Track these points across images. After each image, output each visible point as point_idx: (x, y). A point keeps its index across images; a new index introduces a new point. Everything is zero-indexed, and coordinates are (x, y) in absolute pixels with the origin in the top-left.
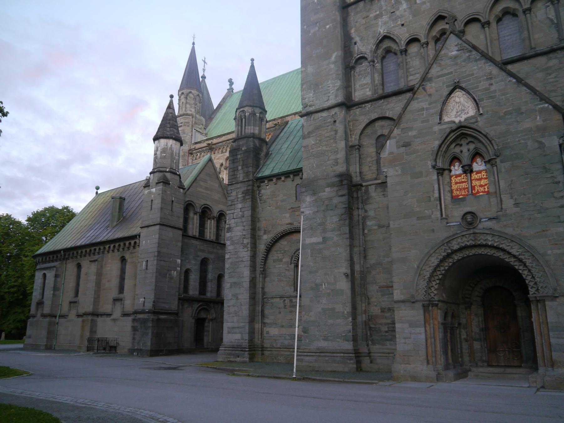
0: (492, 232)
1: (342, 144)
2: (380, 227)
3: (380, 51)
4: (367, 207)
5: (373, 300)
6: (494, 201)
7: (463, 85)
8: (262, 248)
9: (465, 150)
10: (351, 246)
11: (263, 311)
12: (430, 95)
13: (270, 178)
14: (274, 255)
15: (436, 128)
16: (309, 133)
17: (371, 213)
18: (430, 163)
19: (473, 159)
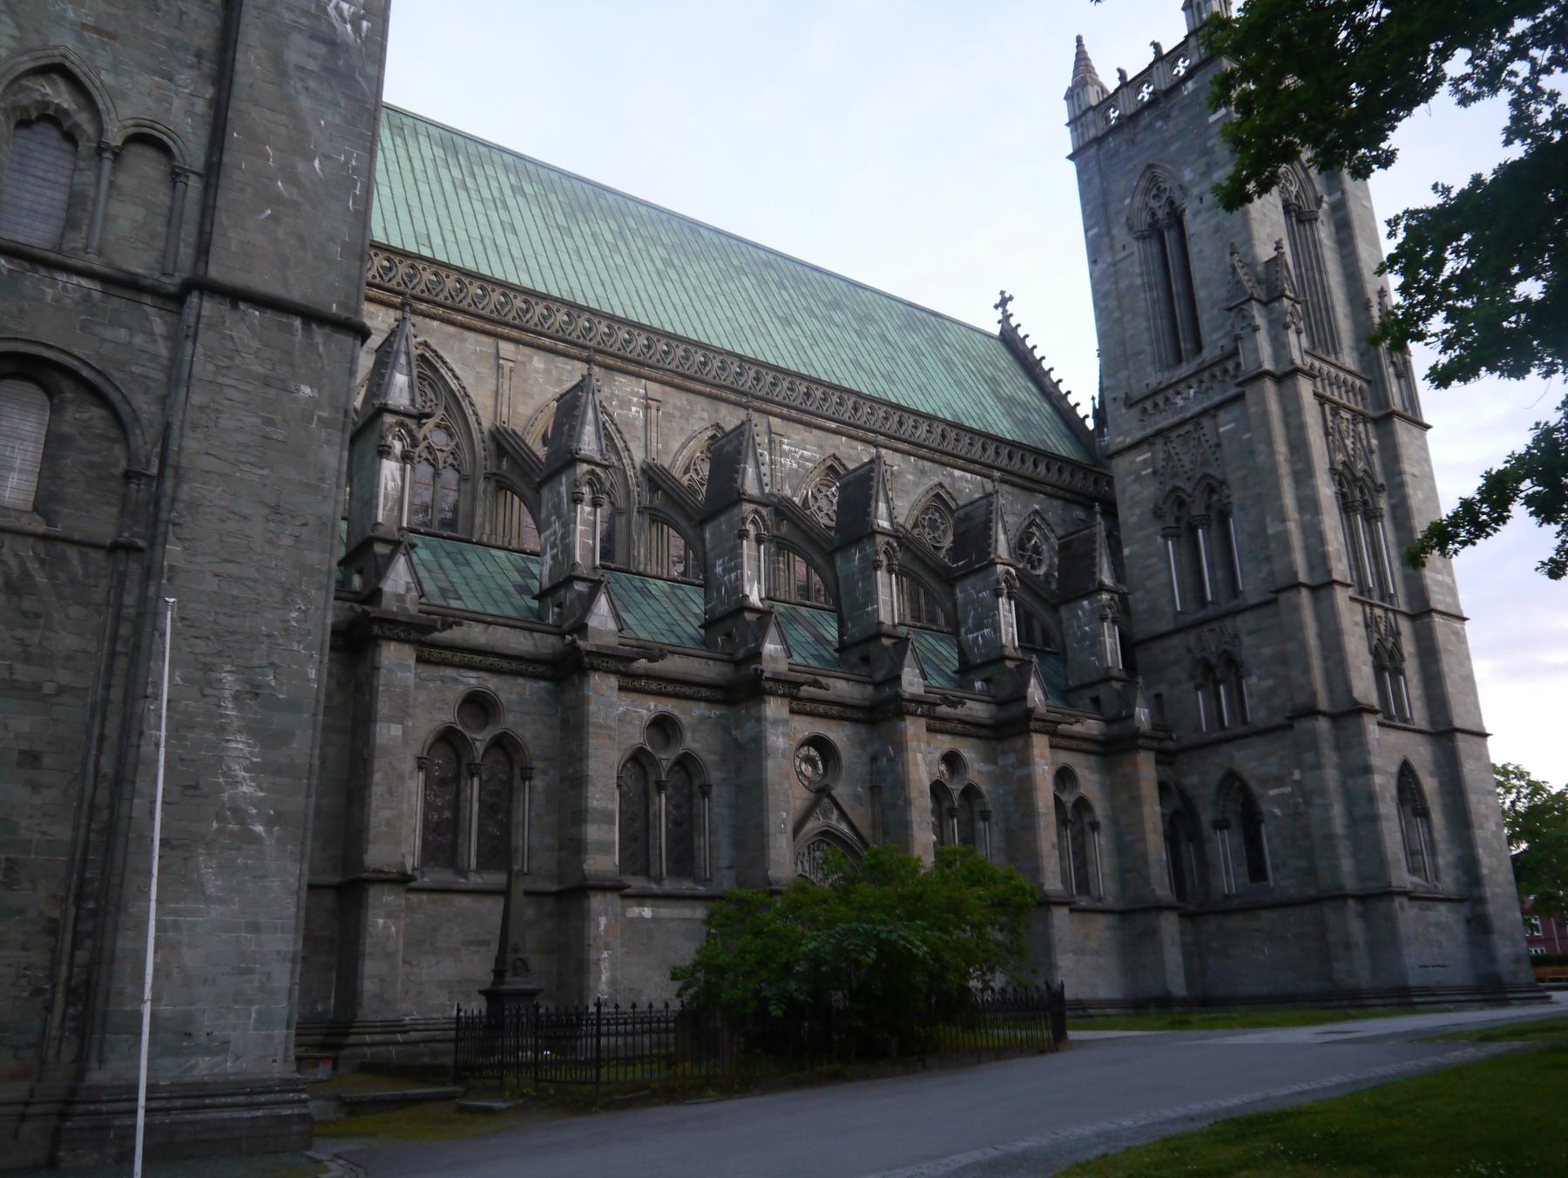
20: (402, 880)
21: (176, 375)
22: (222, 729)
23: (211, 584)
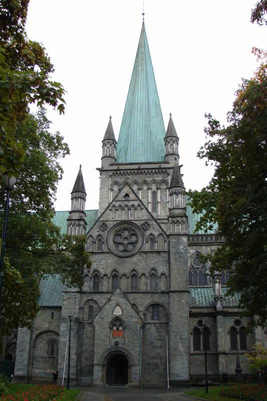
0: (121, 348)
1: (78, 307)
2: (88, 337)
3: (94, 274)
4: (84, 330)
5: (83, 362)
6: (123, 339)
7: (120, 304)
8: (34, 336)
9: (118, 323)
10: (78, 344)
11: (32, 362)
12: (110, 305)
14: (39, 340)
15: (111, 315)
16: (65, 300)
17: (85, 333)
18: (108, 326)
19: (119, 326)
20: (224, 353)
21: (169, 303)
22: (178, 343)
23: (175, 327)
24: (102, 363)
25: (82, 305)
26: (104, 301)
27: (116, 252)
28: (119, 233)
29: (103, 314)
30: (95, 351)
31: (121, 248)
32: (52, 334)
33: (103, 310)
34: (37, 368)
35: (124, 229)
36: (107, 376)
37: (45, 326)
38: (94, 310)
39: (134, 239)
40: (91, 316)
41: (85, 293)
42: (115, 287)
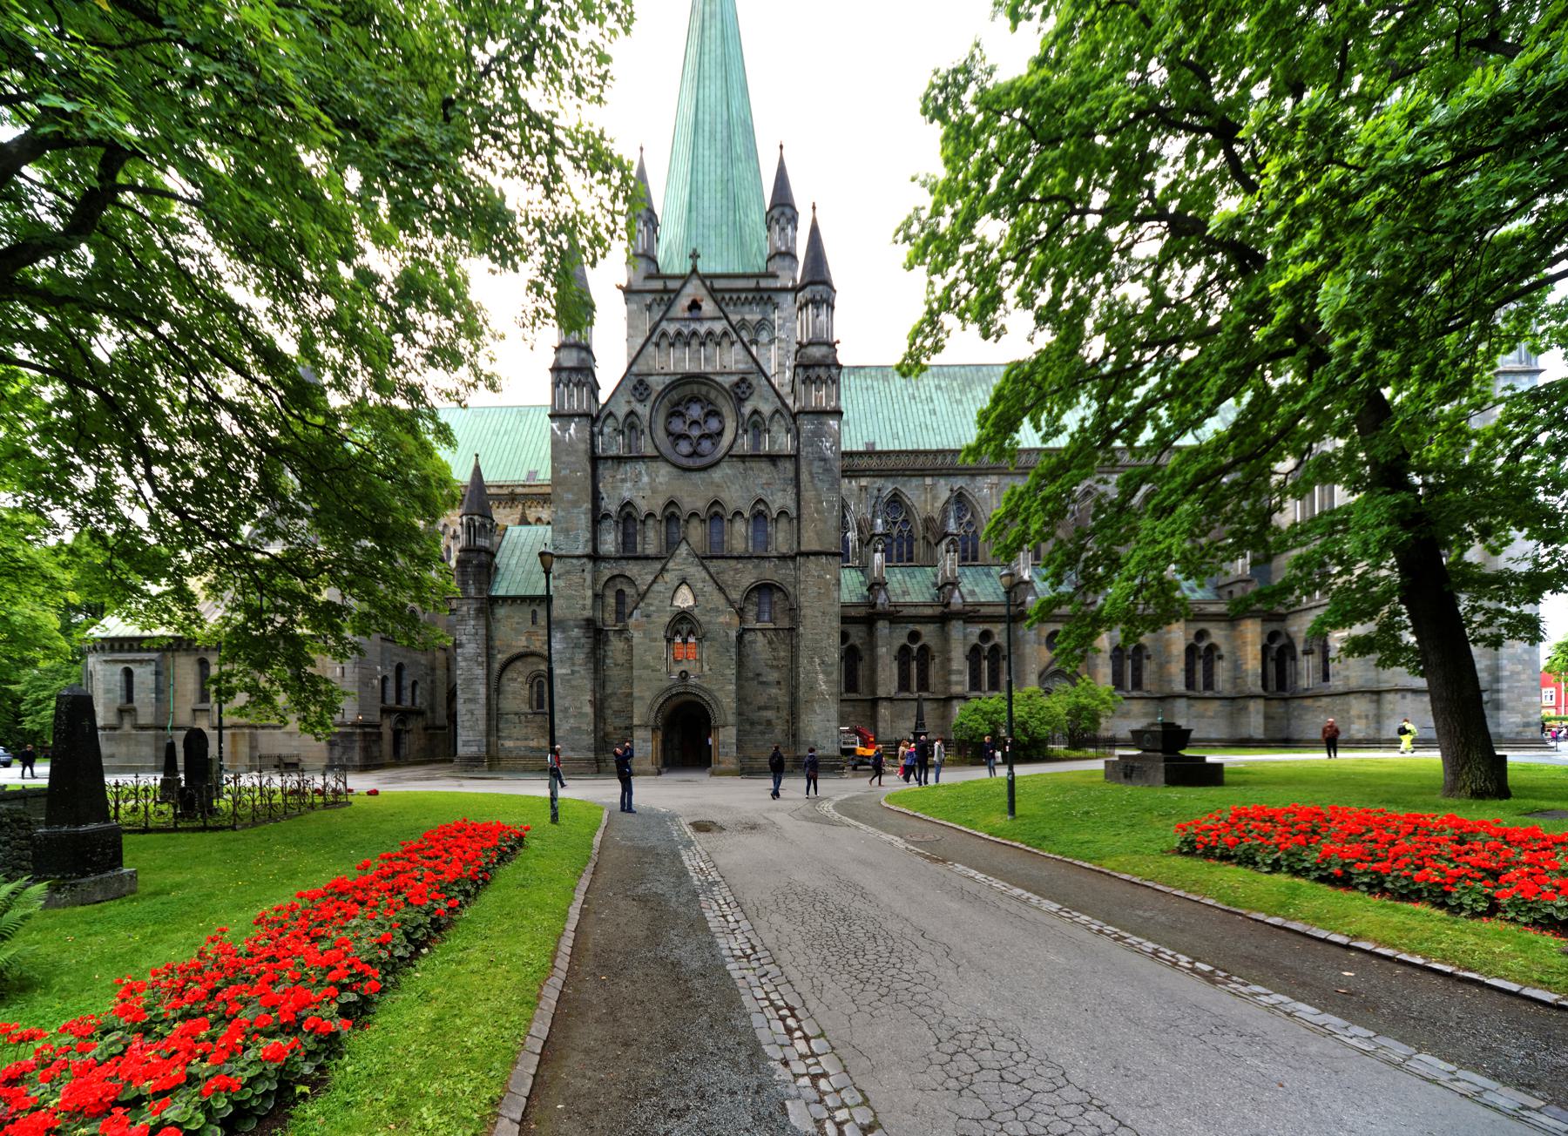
0: (696, 686)
1: (589, 593)
8: (496, 666)
9: (685, 628)
13: (505, 599)
24: (652, 722)
25: (599, 587)
26: (650, 578)
27: (674, 458)
28: (681, 408)
29: (649, 605)
30: (636, 693)
31: (684, 447)
32: (535, 659)
33: (650, 595)
34: (509, 737)
35: (690, 400)
36: (664, 750)
37: (520, 643)
38: (628, 600)
39: (714, 424)
40: (621, 615)
41: (606, 559)
42: (671, 546)
